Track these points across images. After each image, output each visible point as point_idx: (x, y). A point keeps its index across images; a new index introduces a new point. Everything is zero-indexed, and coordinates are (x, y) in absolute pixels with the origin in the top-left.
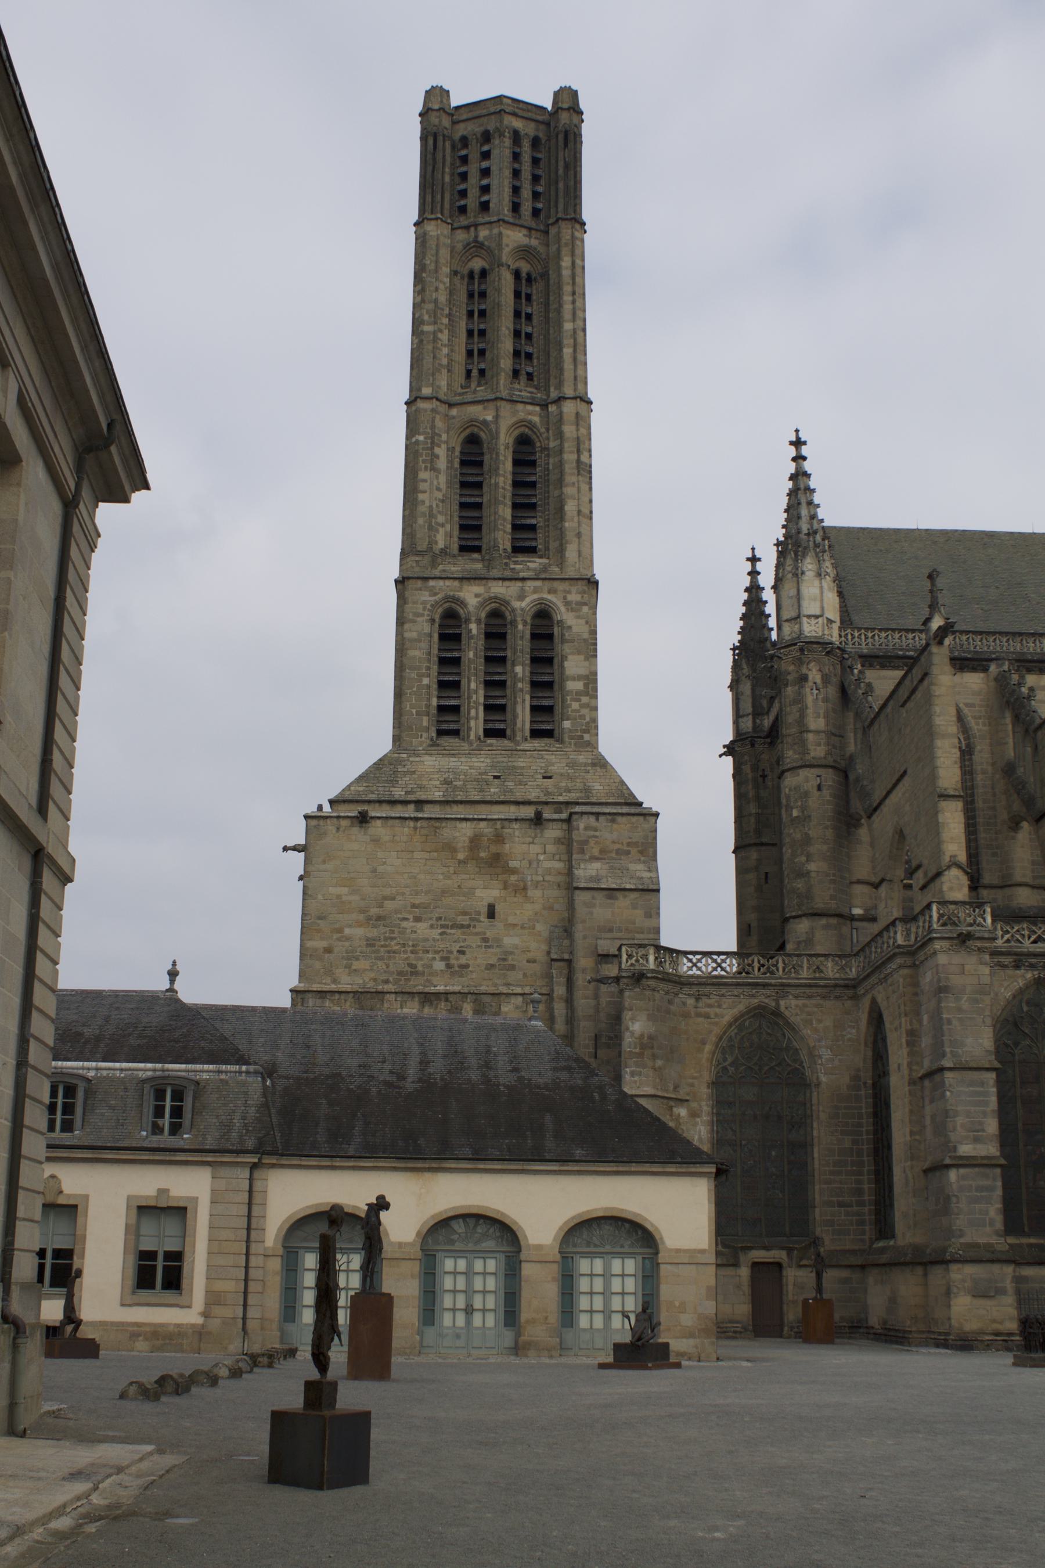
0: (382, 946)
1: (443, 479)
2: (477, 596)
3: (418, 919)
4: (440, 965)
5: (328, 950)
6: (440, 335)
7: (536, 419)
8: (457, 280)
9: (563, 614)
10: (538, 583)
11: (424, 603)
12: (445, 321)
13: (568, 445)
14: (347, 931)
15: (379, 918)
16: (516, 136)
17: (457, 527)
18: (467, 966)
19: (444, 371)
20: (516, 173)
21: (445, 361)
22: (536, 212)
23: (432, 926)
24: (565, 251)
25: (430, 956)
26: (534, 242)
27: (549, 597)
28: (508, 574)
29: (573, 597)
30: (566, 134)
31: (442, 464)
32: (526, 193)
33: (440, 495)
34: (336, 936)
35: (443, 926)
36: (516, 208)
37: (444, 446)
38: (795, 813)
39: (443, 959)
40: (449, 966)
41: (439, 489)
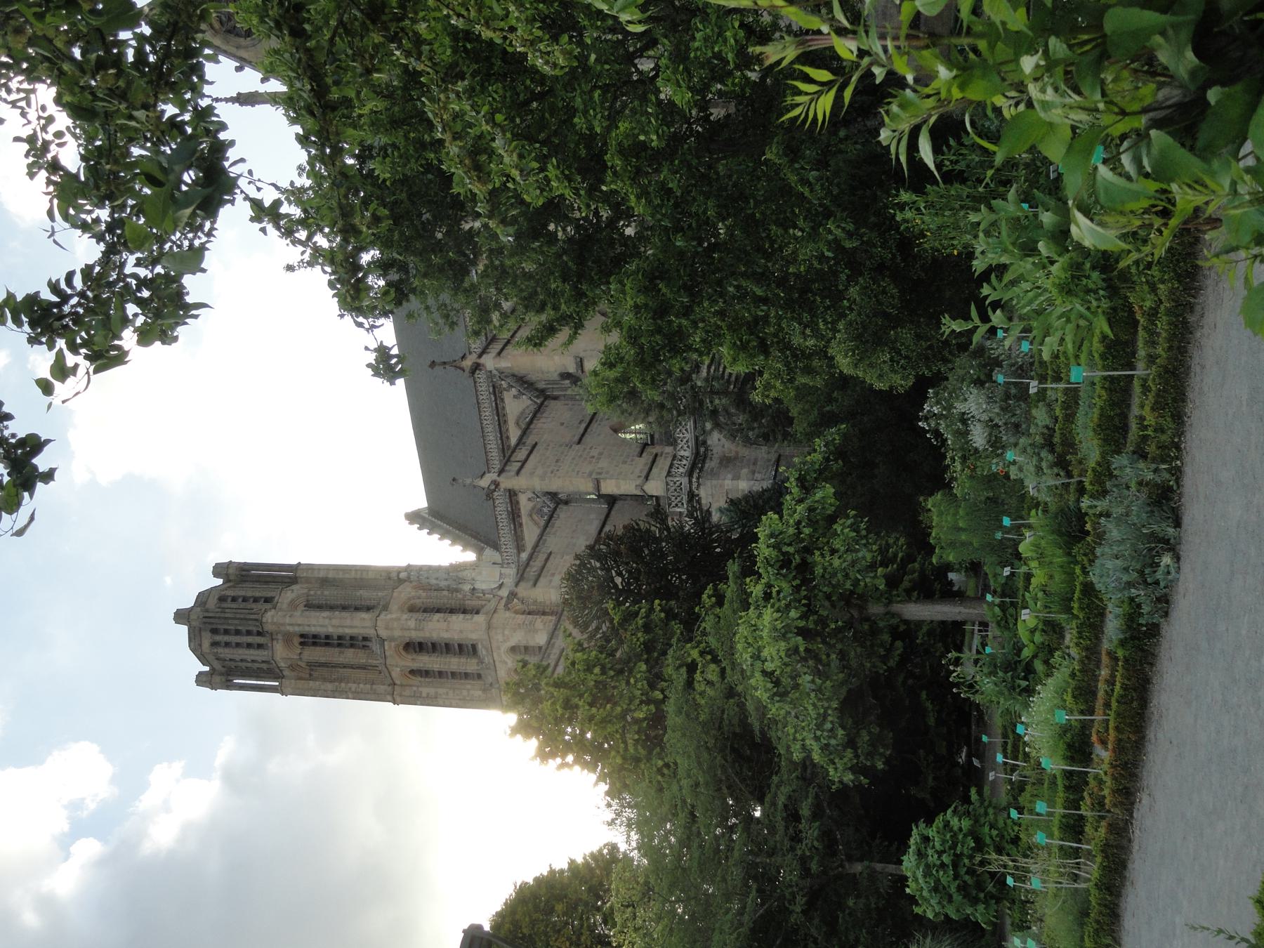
1: (441, 691)
6: (353, 689)
7: (393, 644)
8: (315, 674)
9: (512, 643)
10: (495, 654)
12: (343, 685)
13: (407, 634)
16: (215, 644)
17: (467, 681)
19: (374, 686)
20: (238, 645)
21: (368, 686)
22: (259, 634)
24: (282, 628)
26: (280, 637)
28: (492, 667)
29: (500, 638)
30: (205, 623)
31: (432, 691)
32: (250, 639)
33: (451, 692)
36: (260, 646)
37: (420, 689)
41: (447, 693)
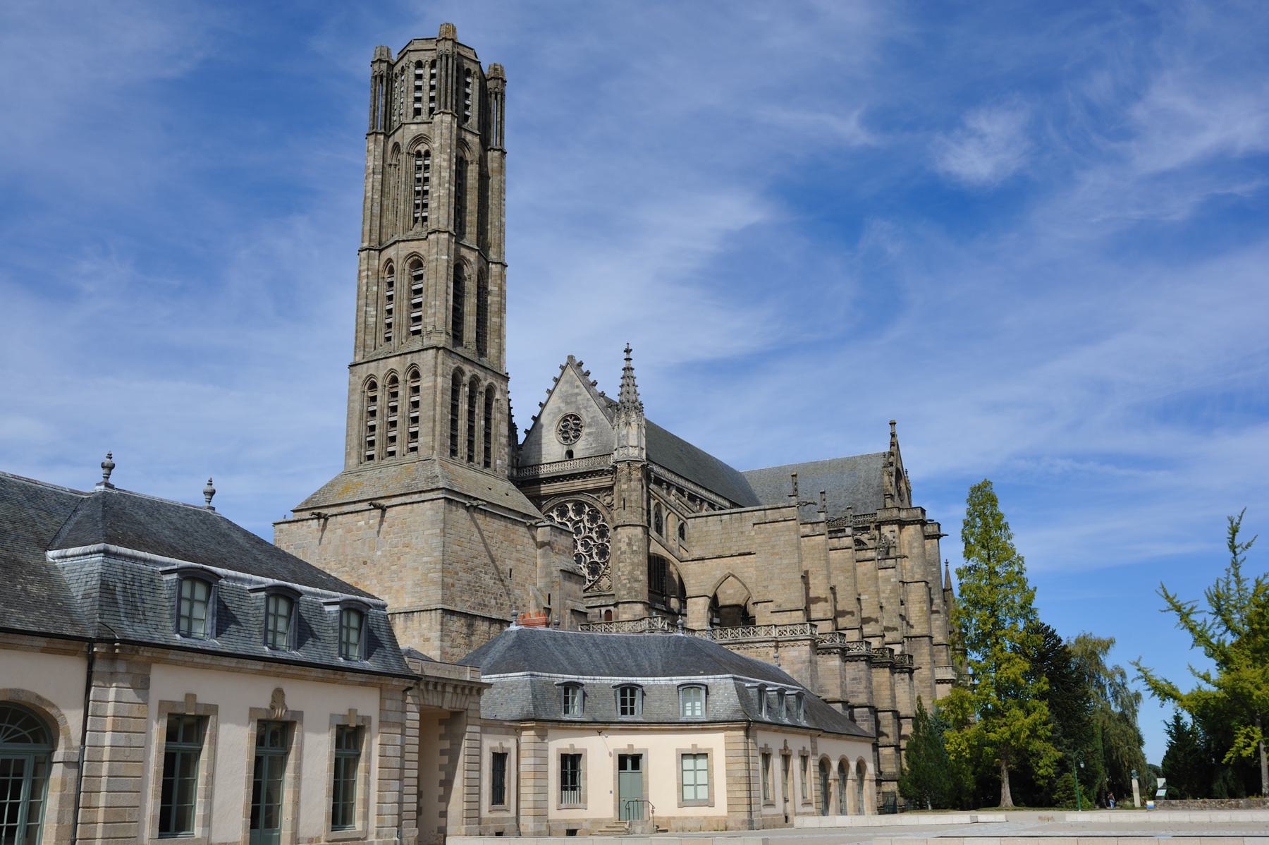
0: (474, 586)
2: (470, 371)
3: (486, 573)
4: (493, 602)
5: (453, 585)
11: (450, 367)
14: (460, 574)
15: (472, 570)
18: (502, 604)
23: (491, 578)
25: (490, 595)
27: (495, 383)
34: (456, 577)
35: (495, 579)
38: (635, 548)
39: (495, 599)
40: (497, 604)
